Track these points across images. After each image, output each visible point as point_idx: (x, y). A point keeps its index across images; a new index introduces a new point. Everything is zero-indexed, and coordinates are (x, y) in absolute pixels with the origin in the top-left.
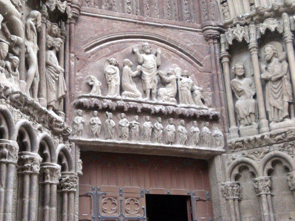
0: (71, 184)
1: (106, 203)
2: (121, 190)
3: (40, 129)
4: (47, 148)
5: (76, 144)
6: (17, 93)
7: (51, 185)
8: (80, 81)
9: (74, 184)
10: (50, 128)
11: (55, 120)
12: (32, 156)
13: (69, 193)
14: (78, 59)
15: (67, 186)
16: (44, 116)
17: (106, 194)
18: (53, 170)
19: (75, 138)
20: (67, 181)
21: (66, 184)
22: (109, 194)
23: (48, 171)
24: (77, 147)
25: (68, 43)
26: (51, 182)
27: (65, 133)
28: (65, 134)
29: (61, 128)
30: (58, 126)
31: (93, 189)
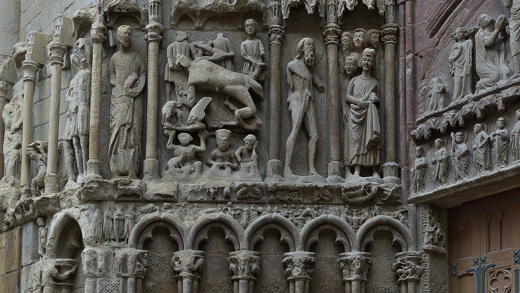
0: (406, 270)
1: (494, 280)
2: (516, 254)
3: (308, 215)
4: (338, 233)
5: (417, 206)
6: (239, 188)
7: (350, 282)
8: (423, 95)
9: (408, 268)
10: (345, 203)
11: (343, 189)
12: (290, 258)
13: (406, 282)
14: (421, 57)
15: (401, 274)
16: (316, 193)
17: (494, 266)
18: (348, 262)
19: (413, 195)
20: (399, 266)
21: (399, 270)
22: (498, 264)
23: (342, 265)
24: (421, 208)
25: (401, 39)
26: (349, 279)
27: (385, 197)
28: (384, 199)
29: (364, 194)
30: (354, 196)
31: (476, 262)
